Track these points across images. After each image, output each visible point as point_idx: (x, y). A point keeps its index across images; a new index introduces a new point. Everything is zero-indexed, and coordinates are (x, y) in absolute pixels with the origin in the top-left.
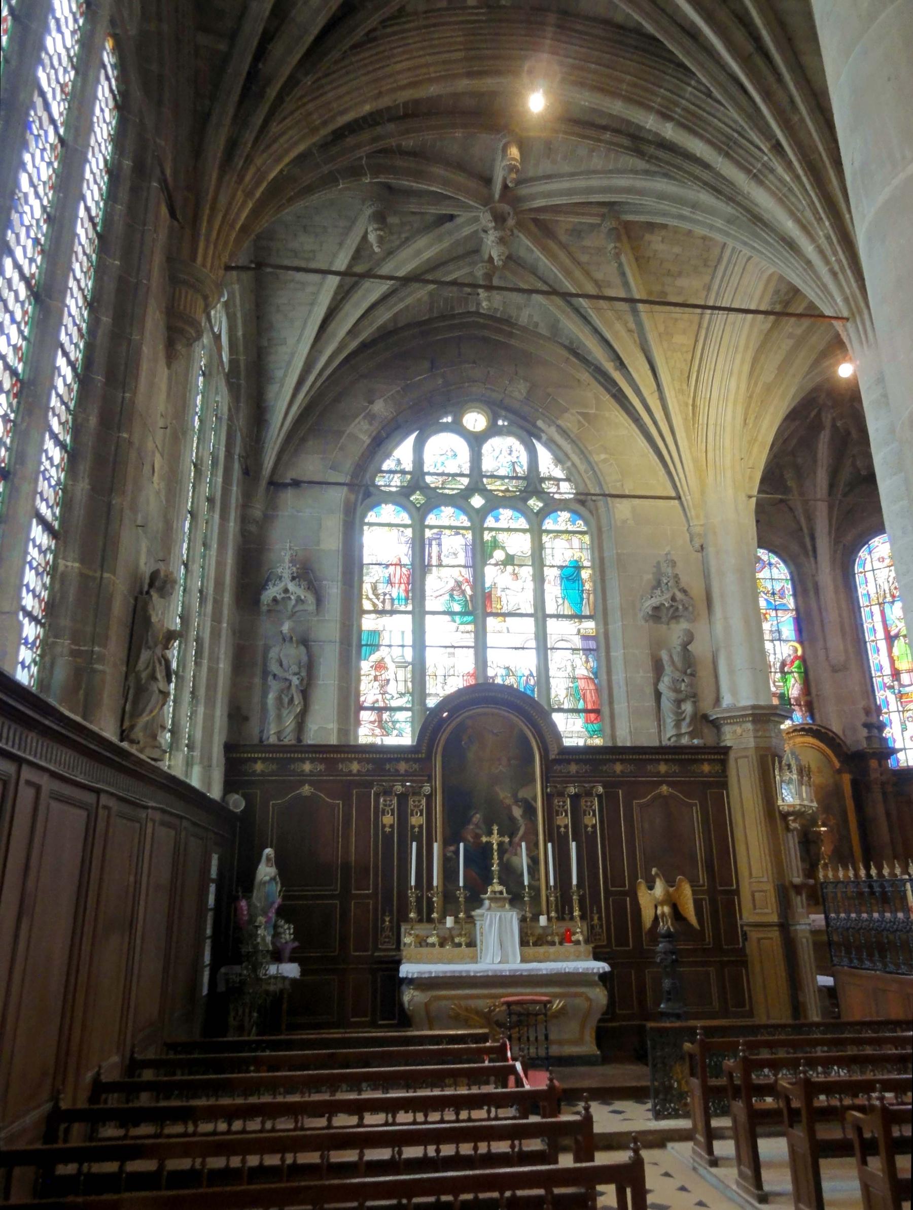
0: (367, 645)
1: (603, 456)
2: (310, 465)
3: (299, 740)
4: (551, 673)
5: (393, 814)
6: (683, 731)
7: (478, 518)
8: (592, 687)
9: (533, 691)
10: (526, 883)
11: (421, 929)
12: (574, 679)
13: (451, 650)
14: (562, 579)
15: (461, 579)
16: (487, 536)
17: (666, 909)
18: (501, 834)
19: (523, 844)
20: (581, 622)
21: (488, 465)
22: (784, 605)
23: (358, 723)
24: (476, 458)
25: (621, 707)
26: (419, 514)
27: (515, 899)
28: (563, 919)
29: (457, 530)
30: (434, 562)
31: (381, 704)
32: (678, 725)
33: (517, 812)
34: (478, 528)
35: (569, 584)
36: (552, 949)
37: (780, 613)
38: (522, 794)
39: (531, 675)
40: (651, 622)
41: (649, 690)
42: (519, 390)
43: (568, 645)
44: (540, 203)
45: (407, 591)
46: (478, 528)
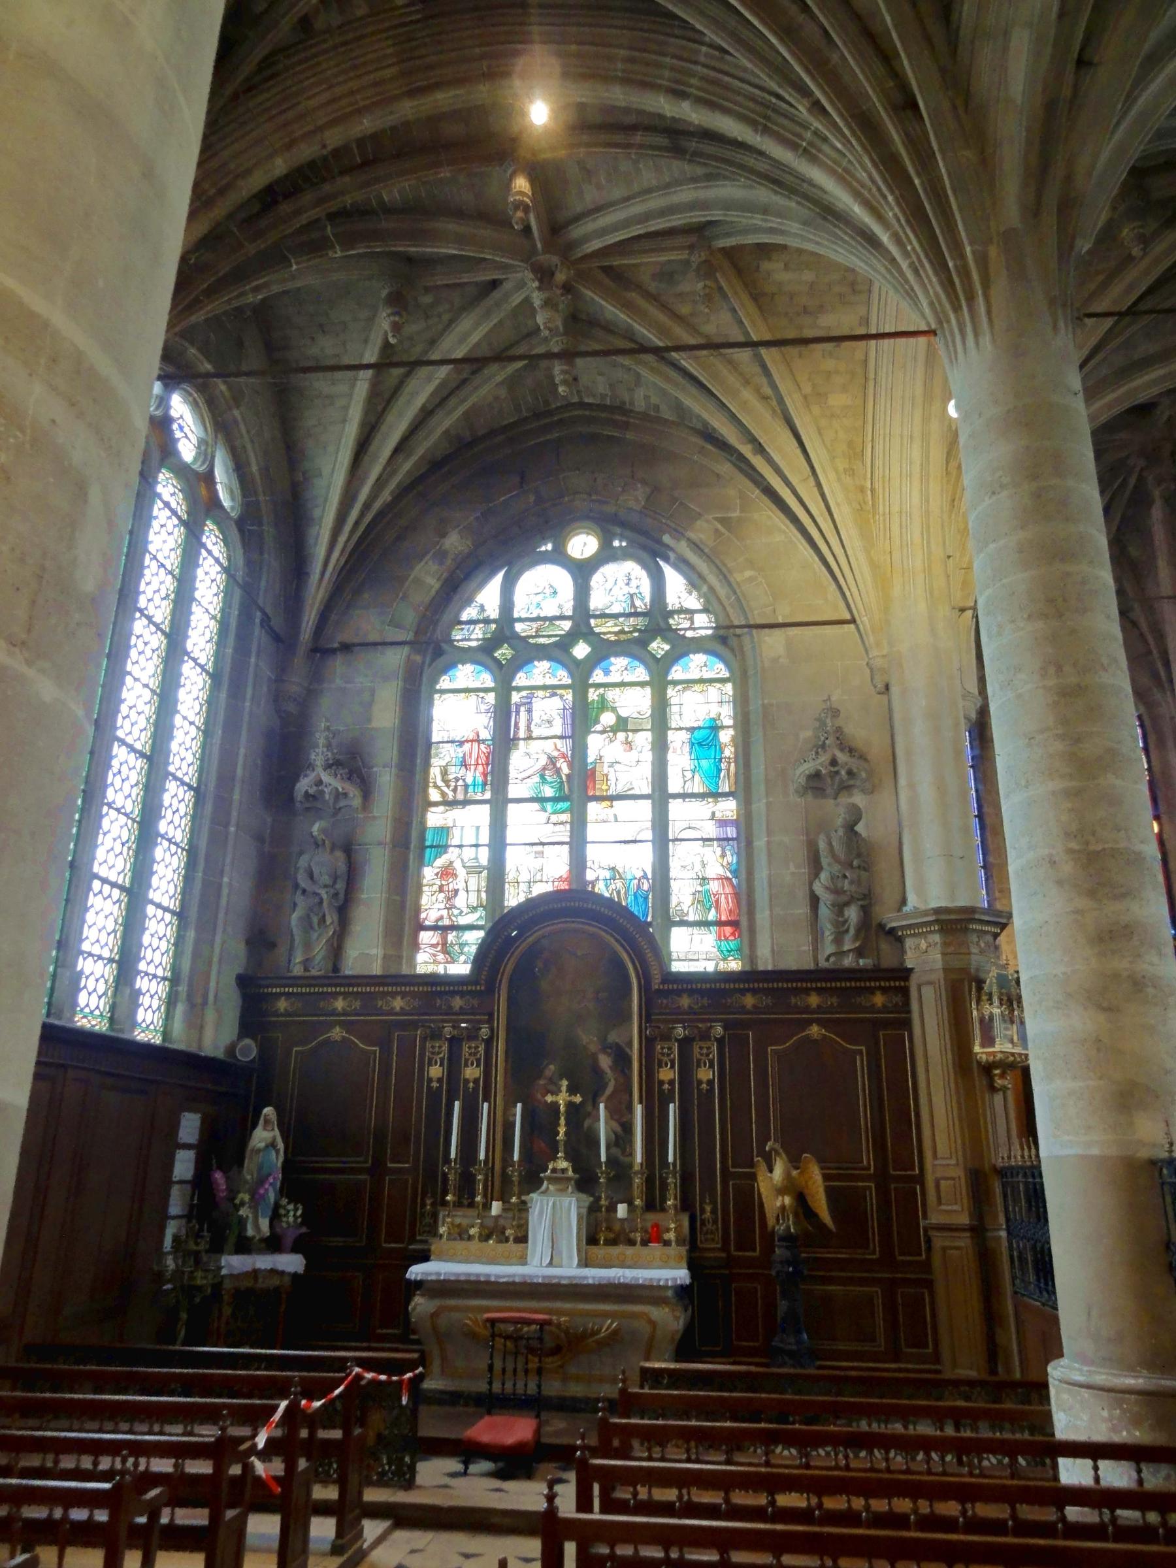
0: (432, 847)
1: (748, 573)
2: (367, 622)
3: (336, 969)
4: (672, 874)
5: (712, 1066)
6: (846, 948)
7: (581, 673)
8: (728, 890)
9: (646, 898)
11: (461, 1217)
12: (704, 880)
13: (540, 848)
14: (692, 745)
15: (556, 754)
16: (593, 695)
17: (787, 1200)
18: (572, 1090)
20: (716, 802)
21: (597, 601)
23: (415, 946)
24: (582, 592)
25: (763, 917)
26: (504, 675)
27: (585, 1182)
29: (552, 690)
30: (522, 734)
31: (446, 922)
32: (838, 940)
33: (605, 1062)
34: (581, 685)
35: (701, 752)
36: (630, 1251)
38: (613, 1037)
39: (645, 876)
40: (810, 797)
41: (802, 895)
42: (634, 499)
43: (697, 835)
44: (596, 245)
45: (485, 775)
46: (581, 685)
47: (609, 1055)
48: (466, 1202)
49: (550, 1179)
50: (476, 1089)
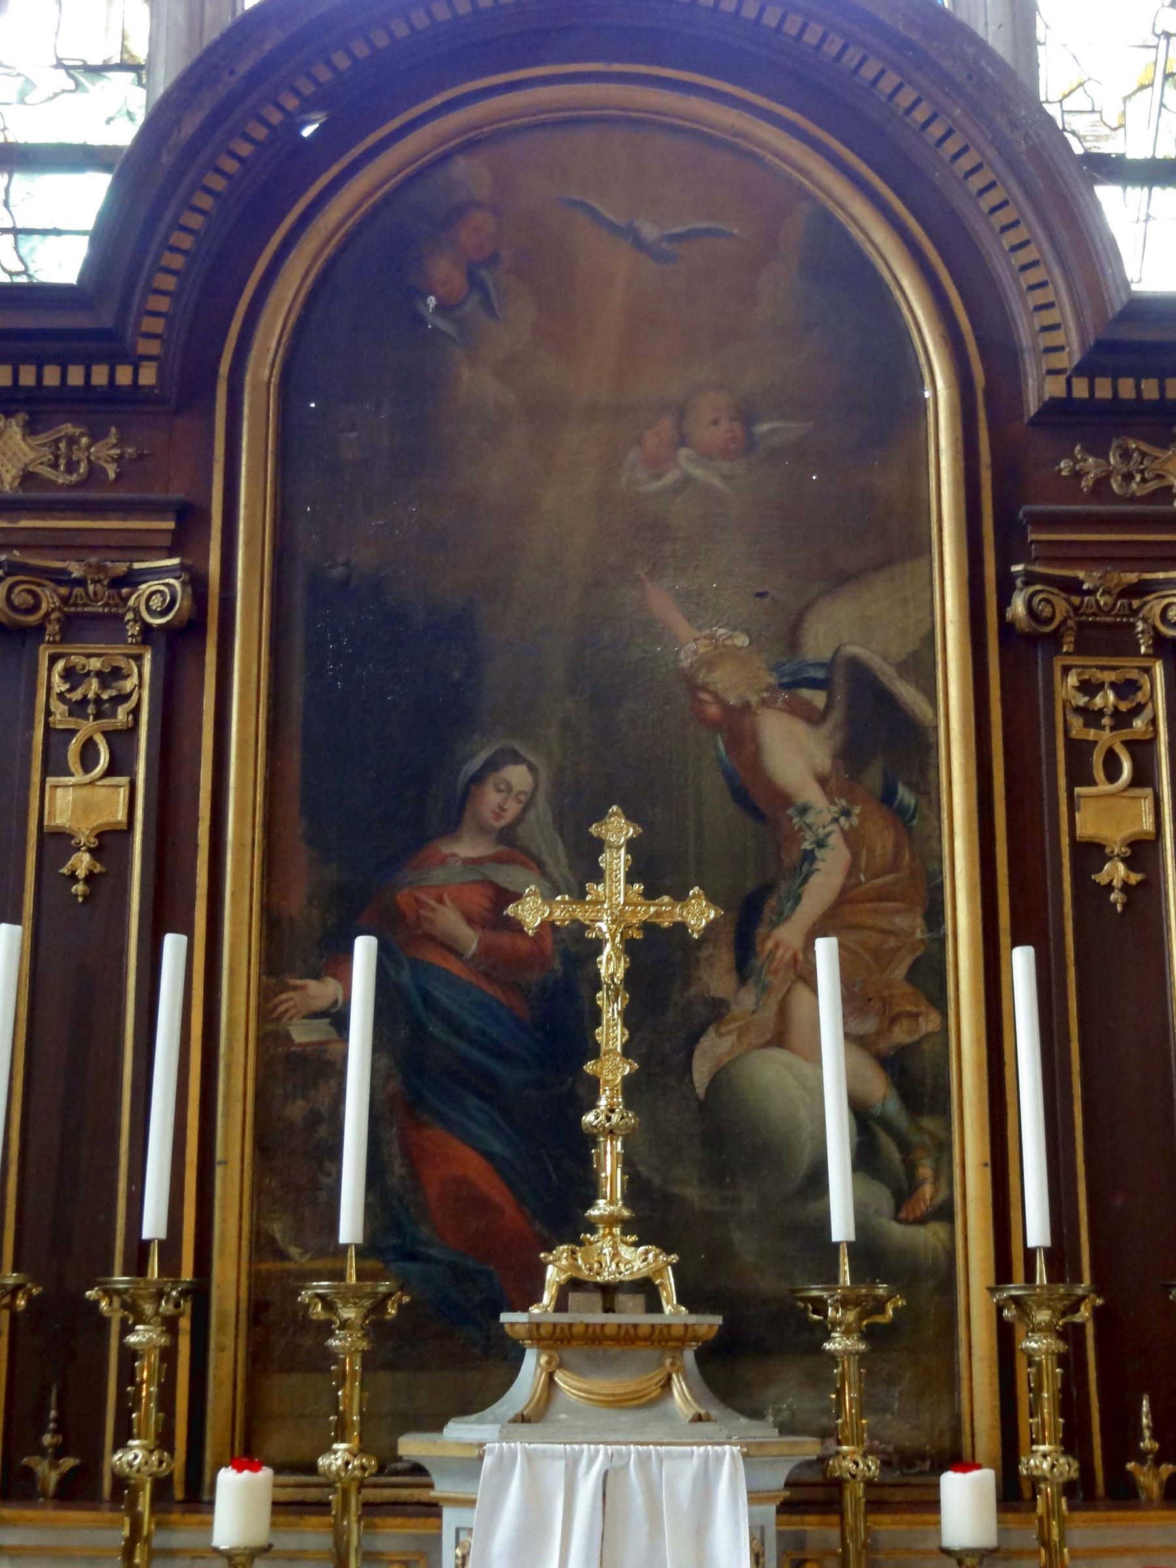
10: (841, 1228)
18: (651, 873)
19: (826, 951)
27: (745, 1352)
28: (1123, 1493)
33: (795, 754)
38: (837, 629)
47: (814, 718)
48: (49, 1475)
49: (556, 1340)
50: (107, 883)
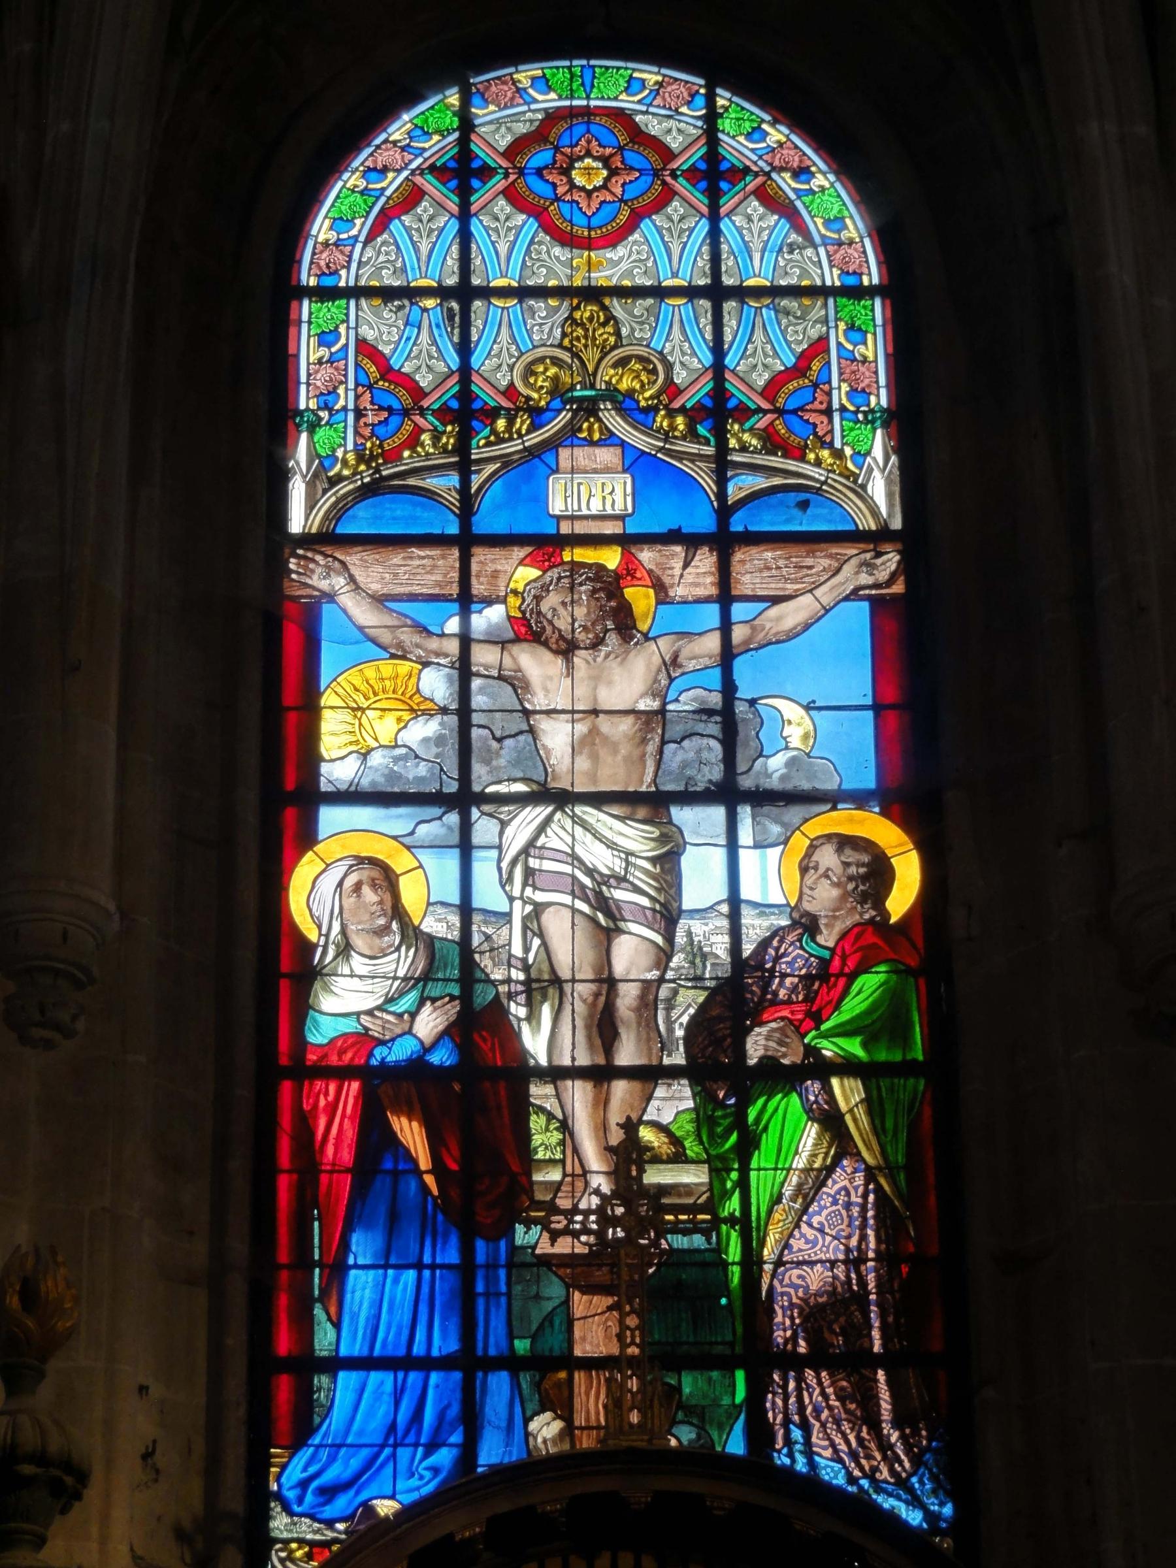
22: (805, 495)
37: (754, 569)
